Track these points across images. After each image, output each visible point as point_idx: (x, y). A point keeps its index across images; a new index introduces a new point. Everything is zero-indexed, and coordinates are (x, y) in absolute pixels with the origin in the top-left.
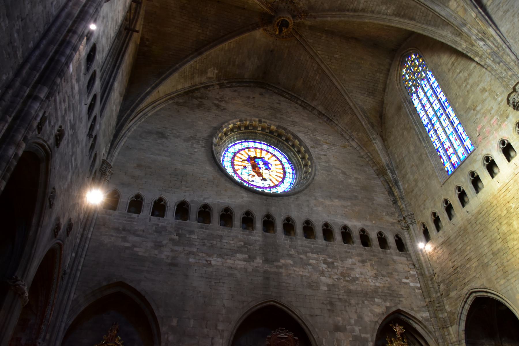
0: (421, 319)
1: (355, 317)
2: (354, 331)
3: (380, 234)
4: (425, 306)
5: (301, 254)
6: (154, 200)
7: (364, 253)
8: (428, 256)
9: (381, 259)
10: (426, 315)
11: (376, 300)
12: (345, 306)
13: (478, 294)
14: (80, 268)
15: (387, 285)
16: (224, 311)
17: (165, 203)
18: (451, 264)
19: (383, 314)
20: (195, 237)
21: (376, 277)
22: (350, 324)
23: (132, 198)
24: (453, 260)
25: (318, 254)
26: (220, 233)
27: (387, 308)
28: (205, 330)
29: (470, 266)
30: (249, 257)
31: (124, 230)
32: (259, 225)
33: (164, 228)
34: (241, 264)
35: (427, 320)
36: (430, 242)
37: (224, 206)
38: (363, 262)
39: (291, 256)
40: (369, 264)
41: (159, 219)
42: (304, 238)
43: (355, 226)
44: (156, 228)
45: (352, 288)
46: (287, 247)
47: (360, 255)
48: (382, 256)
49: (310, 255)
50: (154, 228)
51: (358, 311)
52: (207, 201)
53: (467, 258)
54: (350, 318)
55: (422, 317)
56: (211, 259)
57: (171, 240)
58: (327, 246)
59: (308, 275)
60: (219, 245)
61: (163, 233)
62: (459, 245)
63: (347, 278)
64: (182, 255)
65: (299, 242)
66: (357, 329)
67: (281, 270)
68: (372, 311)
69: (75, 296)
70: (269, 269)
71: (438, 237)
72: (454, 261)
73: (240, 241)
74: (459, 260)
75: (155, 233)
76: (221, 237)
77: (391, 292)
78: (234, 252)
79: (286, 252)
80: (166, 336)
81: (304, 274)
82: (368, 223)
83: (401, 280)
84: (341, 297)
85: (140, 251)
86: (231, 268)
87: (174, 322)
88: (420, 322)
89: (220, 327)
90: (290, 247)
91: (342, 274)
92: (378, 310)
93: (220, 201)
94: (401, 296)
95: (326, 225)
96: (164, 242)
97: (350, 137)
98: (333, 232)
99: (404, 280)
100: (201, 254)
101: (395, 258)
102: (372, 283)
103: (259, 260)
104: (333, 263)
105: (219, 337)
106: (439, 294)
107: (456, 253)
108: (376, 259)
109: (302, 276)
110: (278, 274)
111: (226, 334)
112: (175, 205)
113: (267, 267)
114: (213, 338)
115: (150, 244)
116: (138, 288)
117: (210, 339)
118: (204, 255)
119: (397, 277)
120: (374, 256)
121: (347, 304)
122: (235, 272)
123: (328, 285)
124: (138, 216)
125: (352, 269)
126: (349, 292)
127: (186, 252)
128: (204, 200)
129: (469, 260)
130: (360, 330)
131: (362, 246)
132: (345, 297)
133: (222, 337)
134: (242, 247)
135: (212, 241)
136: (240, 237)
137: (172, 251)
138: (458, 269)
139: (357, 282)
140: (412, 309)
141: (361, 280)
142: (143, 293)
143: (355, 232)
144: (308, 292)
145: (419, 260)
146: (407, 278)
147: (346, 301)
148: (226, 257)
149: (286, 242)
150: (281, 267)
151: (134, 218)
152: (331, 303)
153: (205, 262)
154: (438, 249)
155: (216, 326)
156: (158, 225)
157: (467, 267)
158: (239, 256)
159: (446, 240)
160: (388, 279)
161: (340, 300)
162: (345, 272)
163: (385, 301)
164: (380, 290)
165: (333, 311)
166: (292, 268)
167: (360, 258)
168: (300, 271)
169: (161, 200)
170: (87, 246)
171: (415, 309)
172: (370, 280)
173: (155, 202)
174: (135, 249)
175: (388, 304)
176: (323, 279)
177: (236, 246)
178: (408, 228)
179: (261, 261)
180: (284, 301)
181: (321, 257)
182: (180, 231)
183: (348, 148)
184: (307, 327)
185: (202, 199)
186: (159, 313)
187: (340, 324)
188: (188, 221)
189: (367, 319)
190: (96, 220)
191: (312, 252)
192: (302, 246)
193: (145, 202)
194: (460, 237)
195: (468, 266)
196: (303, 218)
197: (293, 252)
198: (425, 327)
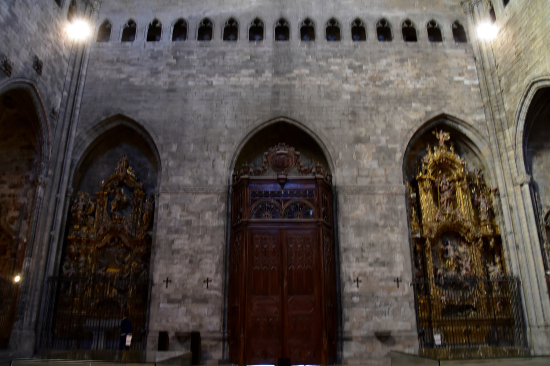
0: (472, 123)
1: (382, 126)
2: (379, 141)
3: (433, 23)
4: (481, 108)
5: (320, 60)
6: (148, 23)
7: (405, 50)
8: (492, 44)
9: (428, 55)
10: (481, 117)
11: (414, 105)
12: (371, 116)
13: (540, 84)
14: (78, 105)
15: (432, 86)
16: (226, 133)
17: (161, 24)
18: (514, 49)
19: (421, 120)
20: (194, 57)
22: (374, 134)
23: (126, 24)
24: (517, 44)
25: (342, 57)
26: (223, 48)
27: (427, 113)
28: (206, 154)
29: (534, 48)
30: (257, 71)
31: (118, 61)
32: (269, 33)
33: (160, 53)
34: (247, 81)
35: (481, 123)
36: (495, 23)
37: (226, 18)
38: (402, 61)
39: (306, 65)
41: (155, 44)
42: (326, 41)
43: (397, 18)
44: (151, 54)
45: (383, 93)
46: (304, 54)
47: (400, 53)
48: (429, 50)
49: (332, 60)
50: (149, 54)
51: (388, 119)
52: (208, 15)
53: (531, 38)
54: (375, 127)
55: (475, 121)
56: (212, 79)
57: (168, 64)
58: (355, 47)
59: (327, 84)
60: (221, 62)
61: (159, 58)
62: (524, 22)
63: (377, 83)
64: (181, 79)
65: (319, 47)
66: (383, 139)
67: (293, 82)
68: (405, 118)
69: (77, 134)
70: (279, 83)
71: (504, 16)
72: (518, 45)
73: (246, 54)
74: (523, 42)
75: (151, 60)
76: (224, 54)
77: (436, 94)
78: (237, 69)
79: (301, 60)
80: (166, 163)
81: (322, 83)
82: (417, 11)
83: (452, 78)
84: (367, 105)
85: (136, 81)
86: (235, 86)
87: (174, 148)
88: (471, 126)
89: (222, 149)
90: (307, 53)
91: (373, 79)
92: (413, 116)
93: (223, 11)
94: (450, 97)
95: (358, 21)
96: (161, 68)
98: (366, 30)
99: (457, 78)
100: (201, 76)
101: (448, 51)
102: (410, 85)
103: (268, 74)
104: (361, 67)
105: (221, 158)
106: (499, 91)
107: (521, 34)
108: (420, 55)
109: (319, 86)
110: (290, 87)
111: (228, 156)
112: (171, 25)
113: (277, 80)
114: (214, 161)
115: (146, 73)
116: (136, 119)
117: (212, 161)
118: (204, 76)
119: (447, 75)
120: (418, 52)
121: (374, 112)
122: (239, 90)
123: (352, 93)
124: (132, 44)
125: (386, 71)
126: (379, 99)
127: (184, 75)
128: (204, 13)
129: (534, 39)
130: (387, 141)
131: (403, 41)
132: (373, 105)
133: (224, 158)
134: (248, 61)
135: (213, 60)
136: (246, 50)
137: (170, 76)
138: (522, 55)
139: (390, 86)
140: (462, 112)
141: (396, 83)
142: (141, 123)
143: (395, 27)
144: (325, 103)
145: (480, 51)
146: (461, 75)
147: (373, 109)
148: (229, 75)
149: (302, 49)
150: (294, 79)
151: (128, 47)
152: (354, 113)
153: (205, 83)
154: (503, 32)
155: (218, 148)
156: (153, 50)
157: (530, 51)
158: (244, 72)
159: (511, 17)
160: (435, 79)
161: (366, 108)
162: (375, 75)
163: (425, 105)
165: (355, 122)
166: (307, 78)
167: (398, 57)
168: (317, 80)
169: (156, 22)
170: (83, 83)
171: (466, 111)
172: (409, 82)
173: (150, 25)
174: (131, 80)
175: (429, 108)
176: (346, 86)
177: (241, 60)
178: (472, 11)
179: (270, 75)
180: (295, 116)
181: (346, 61)
182: (178, 54)
184: (322, 142)
185: (201, 13)
186: (158, 141)
187: (363, 135)
188: (186, 41)
189: (398, 128)
190: (89, 55)
191: (335, 57)
192: (322, 51)
193: (138, 28)
194: (527, 9)
195: (532, 48)
196: (327, 17)
197: (310, 59)
198: (477, 131)
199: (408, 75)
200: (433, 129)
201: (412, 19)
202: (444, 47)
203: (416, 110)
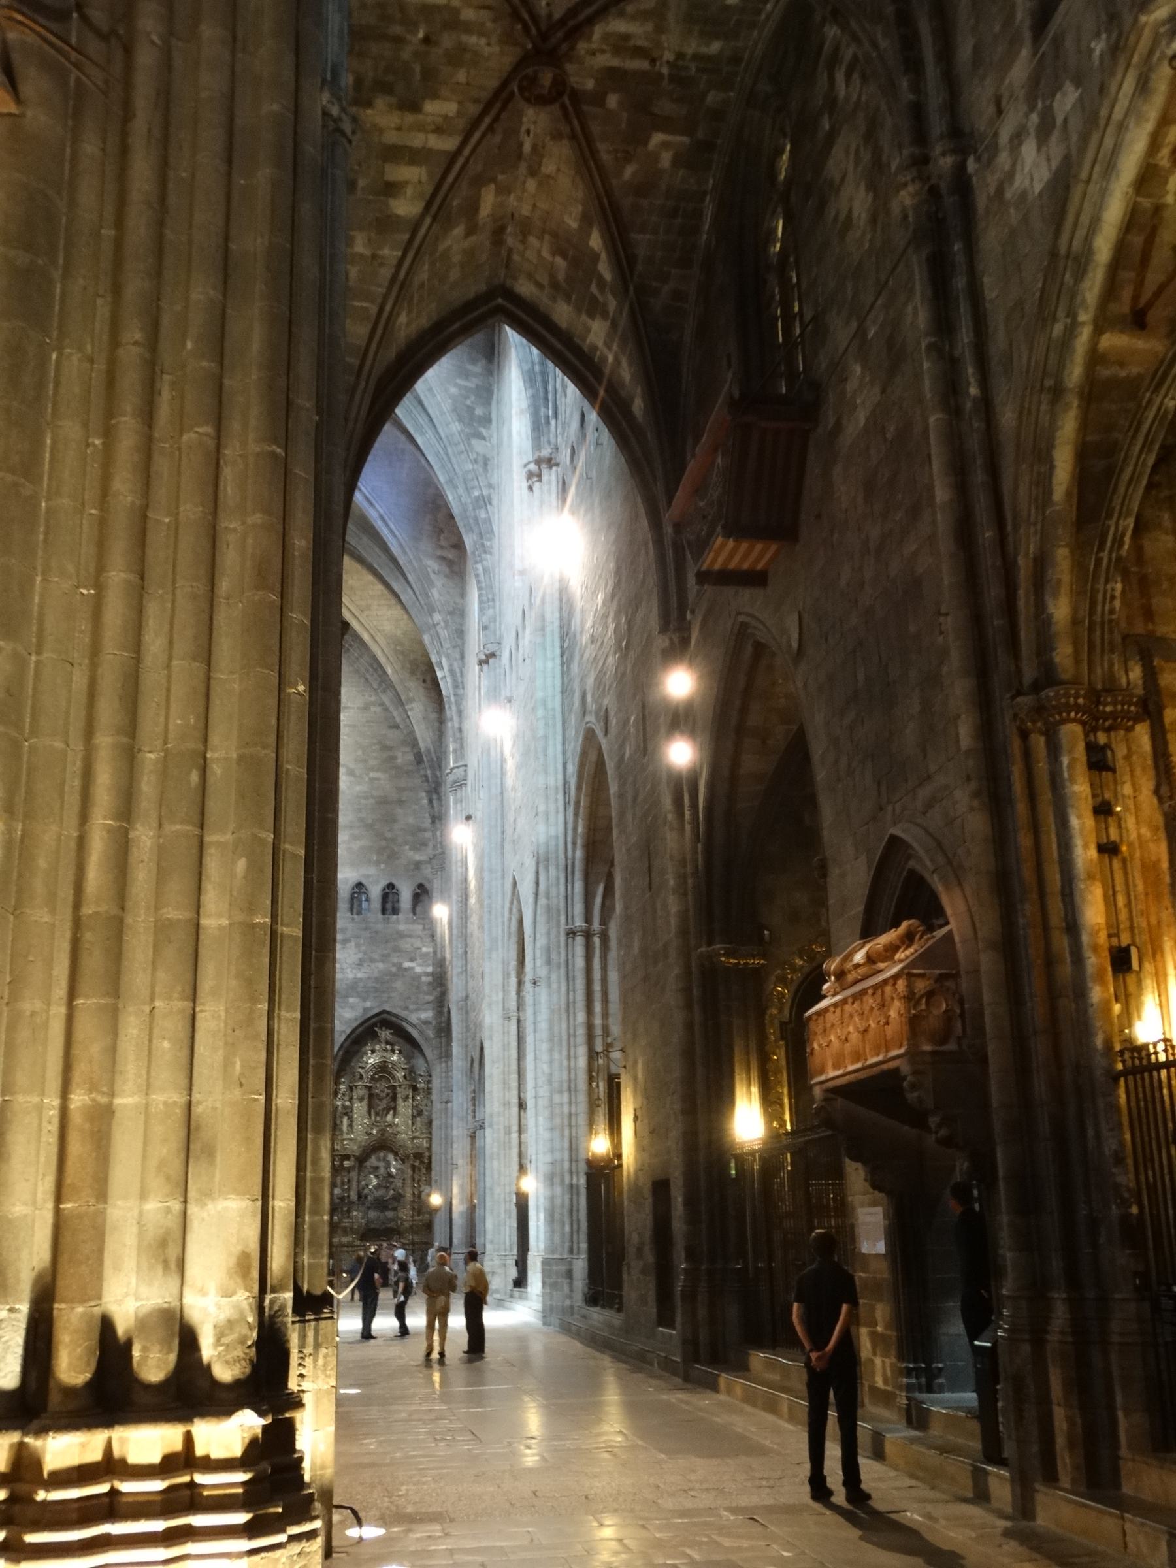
9: (376, 932)
11: (351, 1000)
21: (360, 964)
35: (426, 1023)
40: (353, 944)
55: (419, 1019)
83: (401, 964)
97: (380, 685)
108: (367, 934)
120: (366, 929)
146: (412, 960)
163: (364, 1000)
164: (361, 984)
172: (348, 970)
175: (368, 1004)
183: (373, 709)
199: (349, 961)
200: (375, 1025)
201: (364, 882)
202: (398, 921)
203: (352, 1007)
